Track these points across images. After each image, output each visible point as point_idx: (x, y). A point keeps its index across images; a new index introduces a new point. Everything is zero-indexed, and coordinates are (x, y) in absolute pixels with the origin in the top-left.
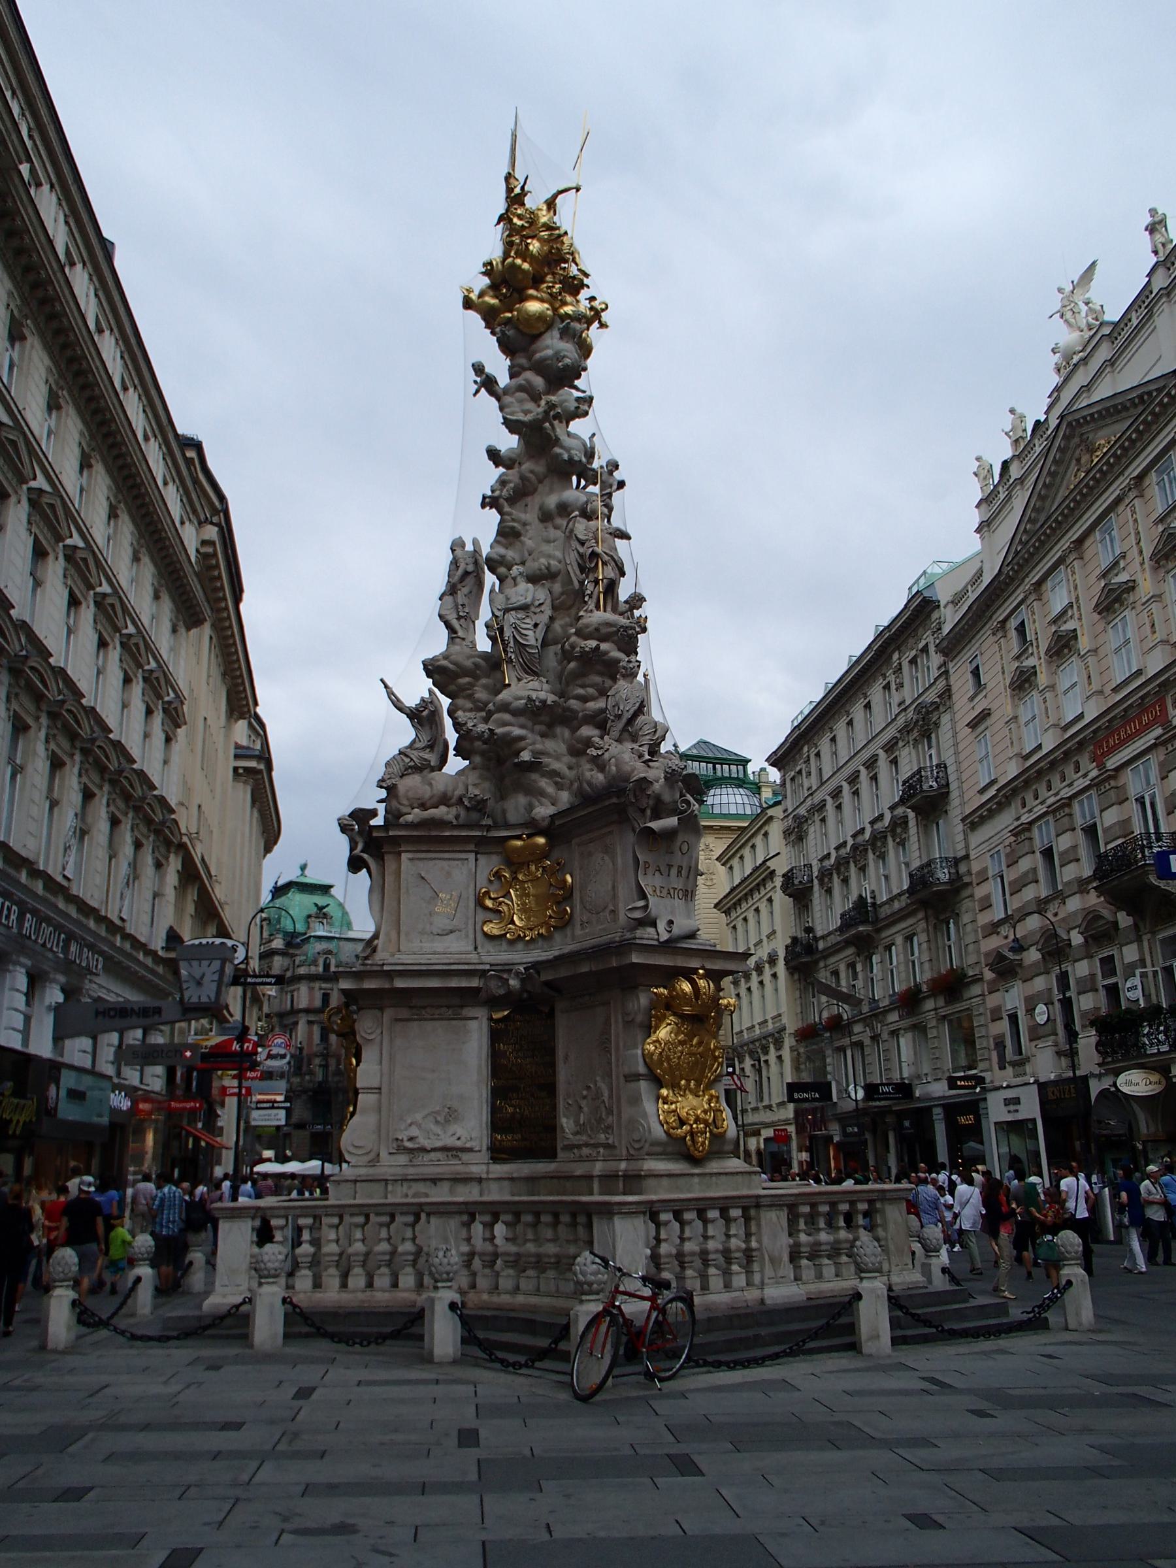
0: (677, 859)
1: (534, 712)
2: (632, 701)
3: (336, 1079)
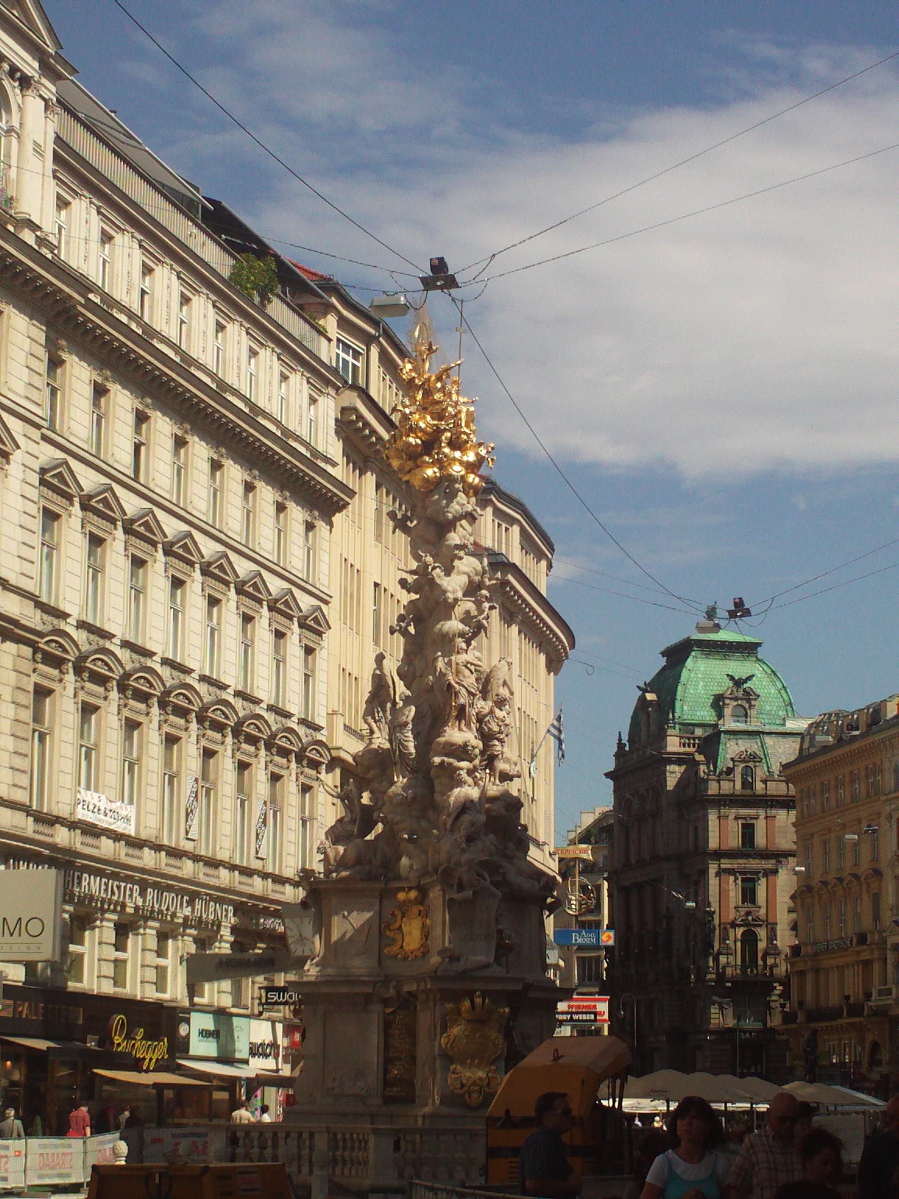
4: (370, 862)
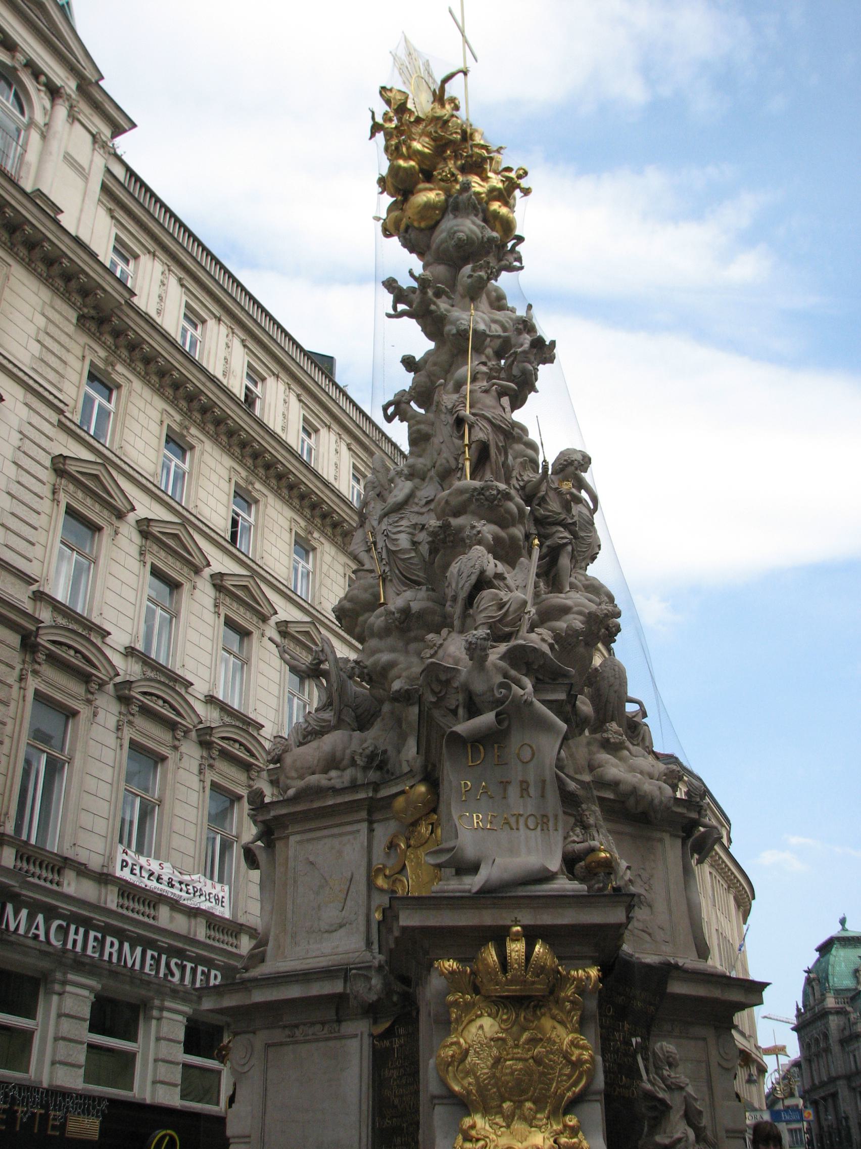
2: (465, 575)
4: (353, 763)
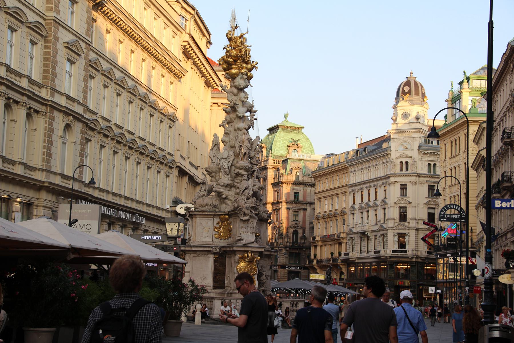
0: (250, 225)
1: (226, 186)
3: (303, 241)
